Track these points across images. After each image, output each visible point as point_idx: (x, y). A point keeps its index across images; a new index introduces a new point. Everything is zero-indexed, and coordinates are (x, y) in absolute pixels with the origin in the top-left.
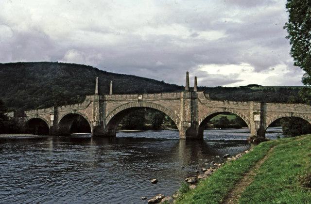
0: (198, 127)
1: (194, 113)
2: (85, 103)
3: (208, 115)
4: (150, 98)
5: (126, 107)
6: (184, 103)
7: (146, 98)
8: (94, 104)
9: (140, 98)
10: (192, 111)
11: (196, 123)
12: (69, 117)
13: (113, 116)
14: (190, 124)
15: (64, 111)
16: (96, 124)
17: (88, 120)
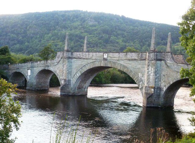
0: (163, 93)
1: (158, 77)
2: (56, 60)
3: (175, 81)
4: (114, 57)
5: (92, 66)
6: (148, 66)
7: (111, 57)
8: (64, 62)
9: (105, 56)
10: (156, 75)
11: (160, 89)
12: (45, 72)
13: (80, 74)
14: (153, 90)
15: (39, 66)
16: (64, 82)
17: (58, 77)
